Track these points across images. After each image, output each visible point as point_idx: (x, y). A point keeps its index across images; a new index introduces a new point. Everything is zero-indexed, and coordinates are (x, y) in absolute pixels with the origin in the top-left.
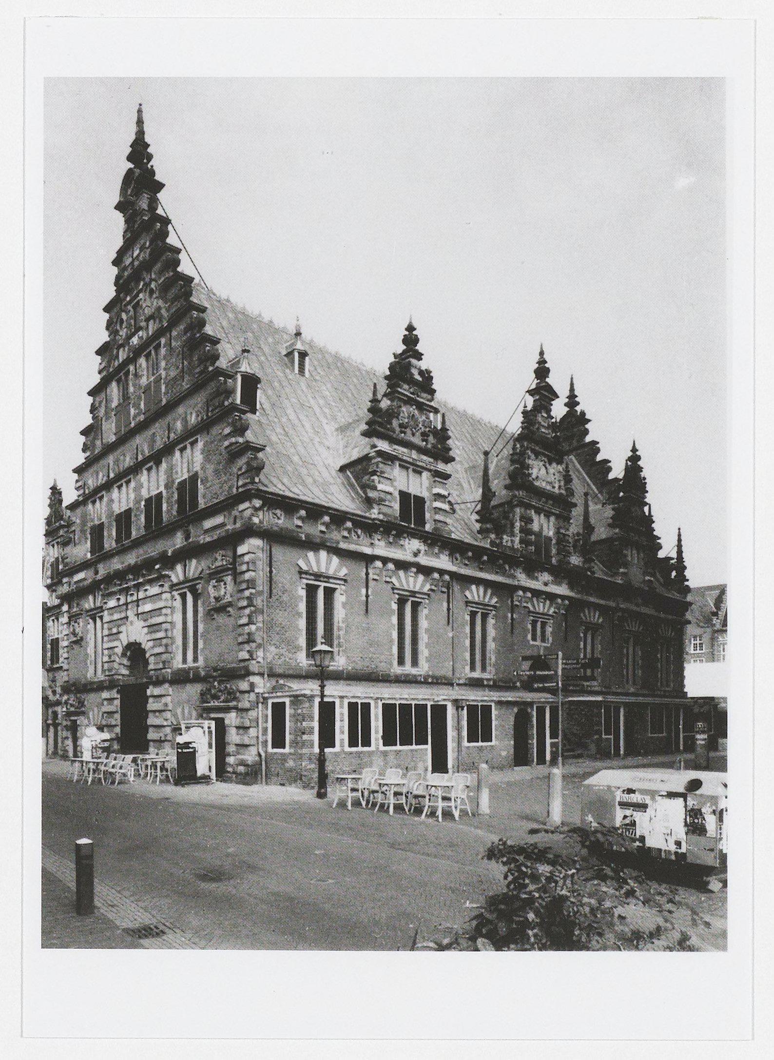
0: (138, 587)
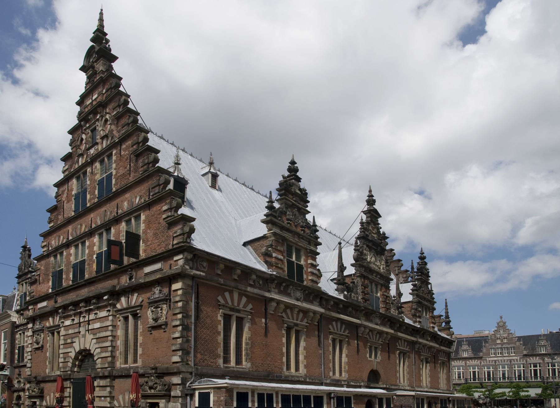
0: (89, 311)
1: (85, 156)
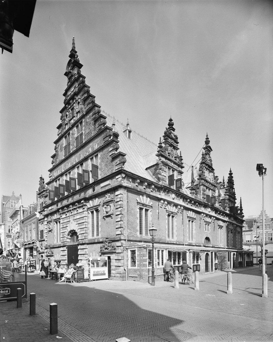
1: (69, 125)
